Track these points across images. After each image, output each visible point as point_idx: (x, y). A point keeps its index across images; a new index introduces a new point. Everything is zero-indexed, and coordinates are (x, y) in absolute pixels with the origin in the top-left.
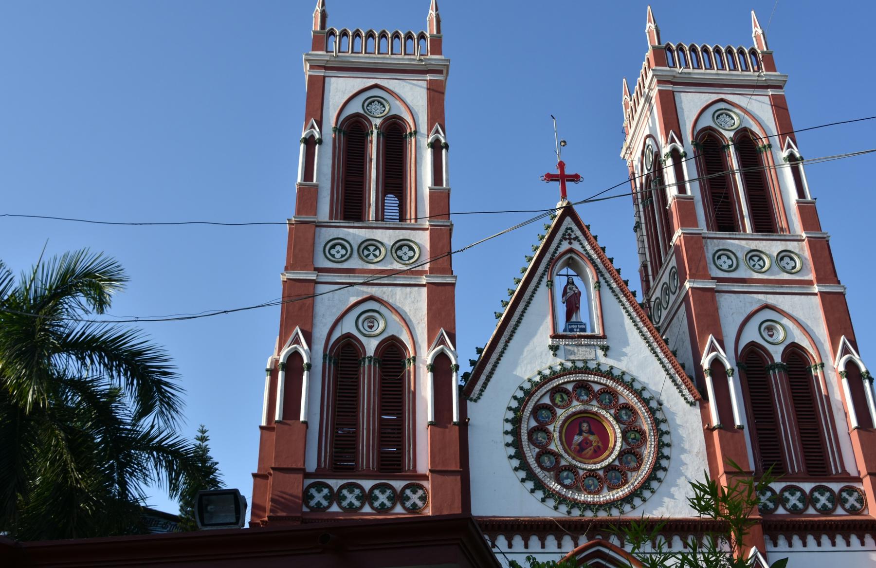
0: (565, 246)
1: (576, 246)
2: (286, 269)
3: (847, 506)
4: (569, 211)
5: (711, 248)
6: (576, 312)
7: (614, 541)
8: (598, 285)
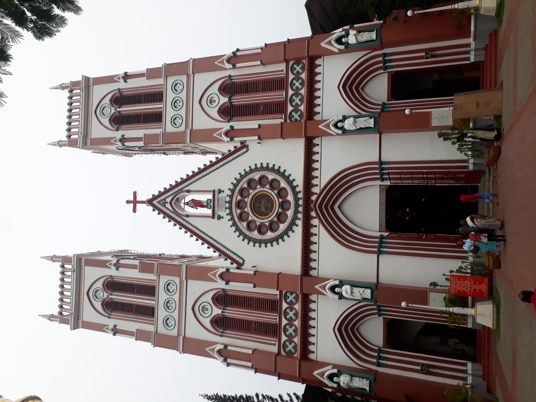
0: (168, 206)
1: (168, 200)
2: (177, 350)
3: (301, 71)
4: (150, 202)
5: (170, 128)
6: (202, 203)
7: (314, 198)
8: (188, 191)
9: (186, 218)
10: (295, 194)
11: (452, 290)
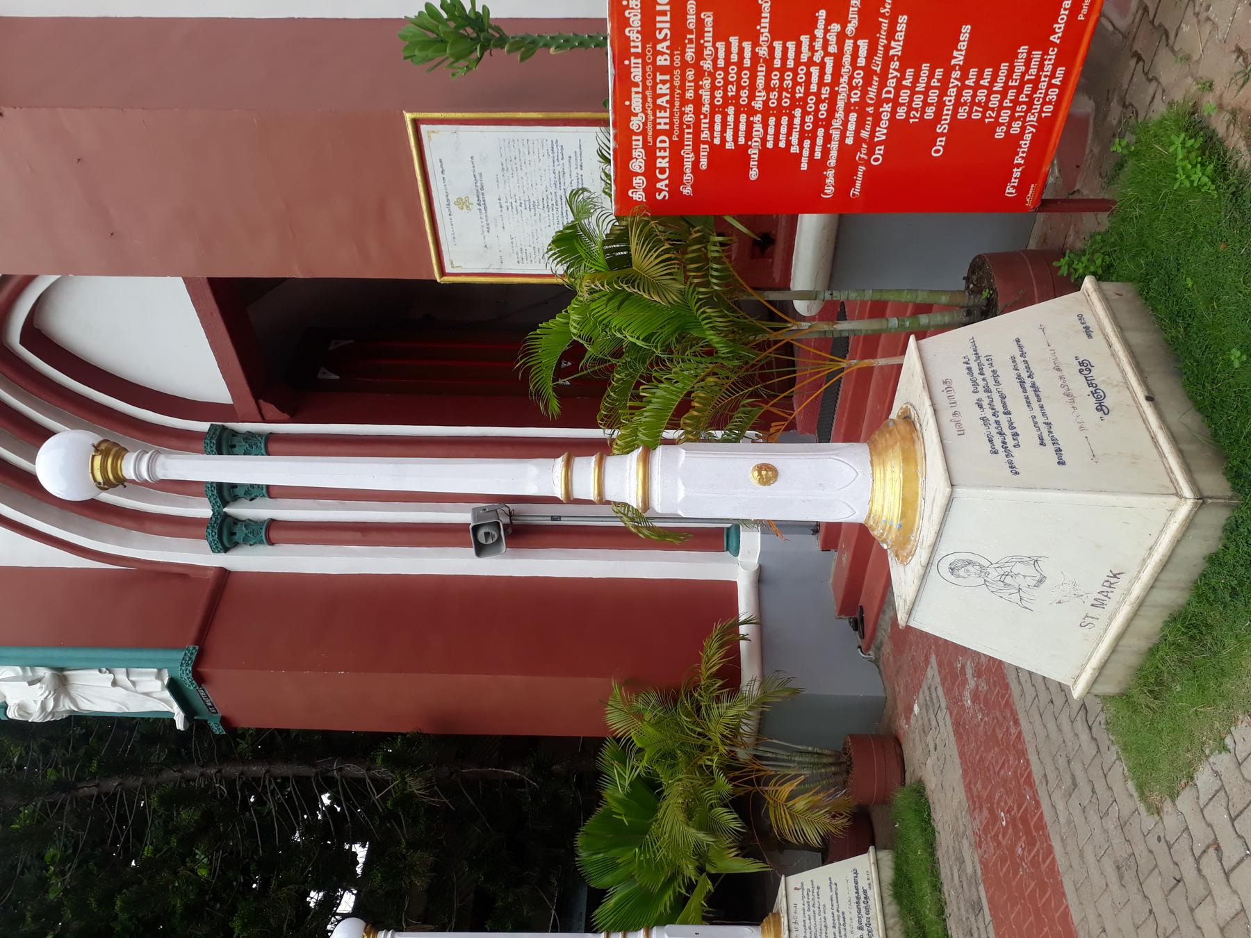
11: (637, 165)
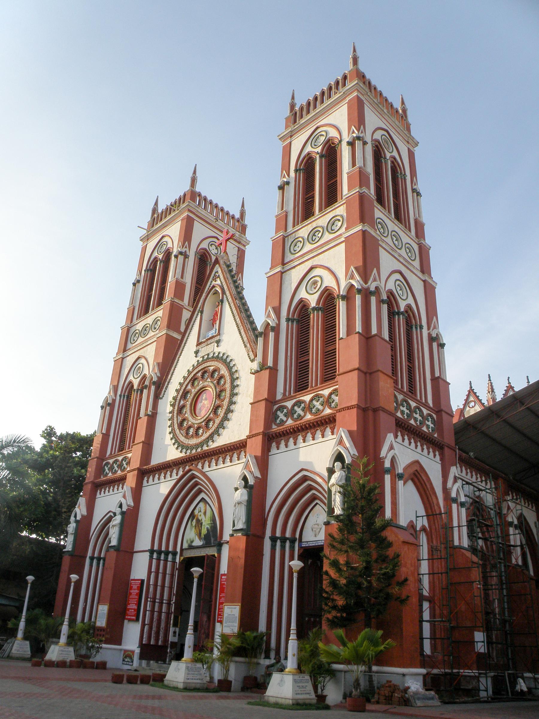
9: (200, 314)
10: (206, 441)
